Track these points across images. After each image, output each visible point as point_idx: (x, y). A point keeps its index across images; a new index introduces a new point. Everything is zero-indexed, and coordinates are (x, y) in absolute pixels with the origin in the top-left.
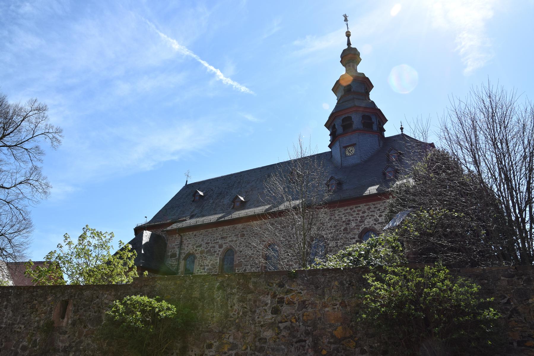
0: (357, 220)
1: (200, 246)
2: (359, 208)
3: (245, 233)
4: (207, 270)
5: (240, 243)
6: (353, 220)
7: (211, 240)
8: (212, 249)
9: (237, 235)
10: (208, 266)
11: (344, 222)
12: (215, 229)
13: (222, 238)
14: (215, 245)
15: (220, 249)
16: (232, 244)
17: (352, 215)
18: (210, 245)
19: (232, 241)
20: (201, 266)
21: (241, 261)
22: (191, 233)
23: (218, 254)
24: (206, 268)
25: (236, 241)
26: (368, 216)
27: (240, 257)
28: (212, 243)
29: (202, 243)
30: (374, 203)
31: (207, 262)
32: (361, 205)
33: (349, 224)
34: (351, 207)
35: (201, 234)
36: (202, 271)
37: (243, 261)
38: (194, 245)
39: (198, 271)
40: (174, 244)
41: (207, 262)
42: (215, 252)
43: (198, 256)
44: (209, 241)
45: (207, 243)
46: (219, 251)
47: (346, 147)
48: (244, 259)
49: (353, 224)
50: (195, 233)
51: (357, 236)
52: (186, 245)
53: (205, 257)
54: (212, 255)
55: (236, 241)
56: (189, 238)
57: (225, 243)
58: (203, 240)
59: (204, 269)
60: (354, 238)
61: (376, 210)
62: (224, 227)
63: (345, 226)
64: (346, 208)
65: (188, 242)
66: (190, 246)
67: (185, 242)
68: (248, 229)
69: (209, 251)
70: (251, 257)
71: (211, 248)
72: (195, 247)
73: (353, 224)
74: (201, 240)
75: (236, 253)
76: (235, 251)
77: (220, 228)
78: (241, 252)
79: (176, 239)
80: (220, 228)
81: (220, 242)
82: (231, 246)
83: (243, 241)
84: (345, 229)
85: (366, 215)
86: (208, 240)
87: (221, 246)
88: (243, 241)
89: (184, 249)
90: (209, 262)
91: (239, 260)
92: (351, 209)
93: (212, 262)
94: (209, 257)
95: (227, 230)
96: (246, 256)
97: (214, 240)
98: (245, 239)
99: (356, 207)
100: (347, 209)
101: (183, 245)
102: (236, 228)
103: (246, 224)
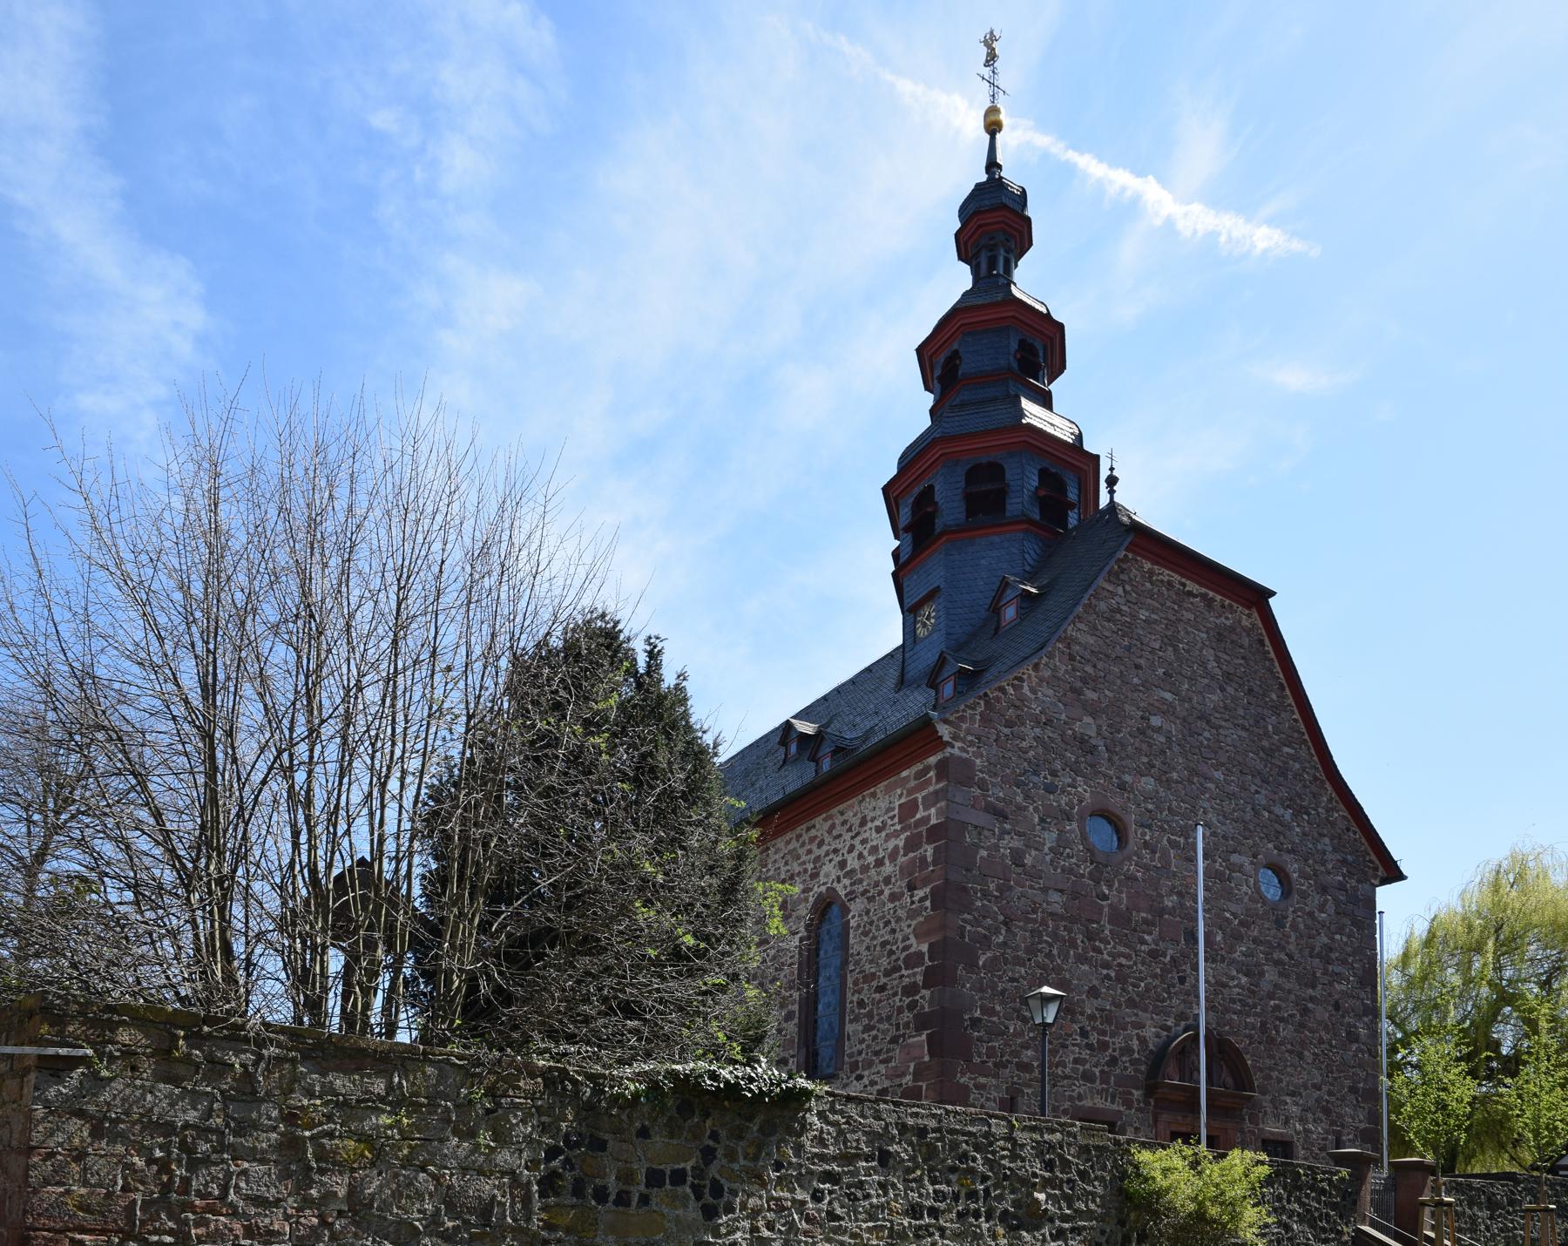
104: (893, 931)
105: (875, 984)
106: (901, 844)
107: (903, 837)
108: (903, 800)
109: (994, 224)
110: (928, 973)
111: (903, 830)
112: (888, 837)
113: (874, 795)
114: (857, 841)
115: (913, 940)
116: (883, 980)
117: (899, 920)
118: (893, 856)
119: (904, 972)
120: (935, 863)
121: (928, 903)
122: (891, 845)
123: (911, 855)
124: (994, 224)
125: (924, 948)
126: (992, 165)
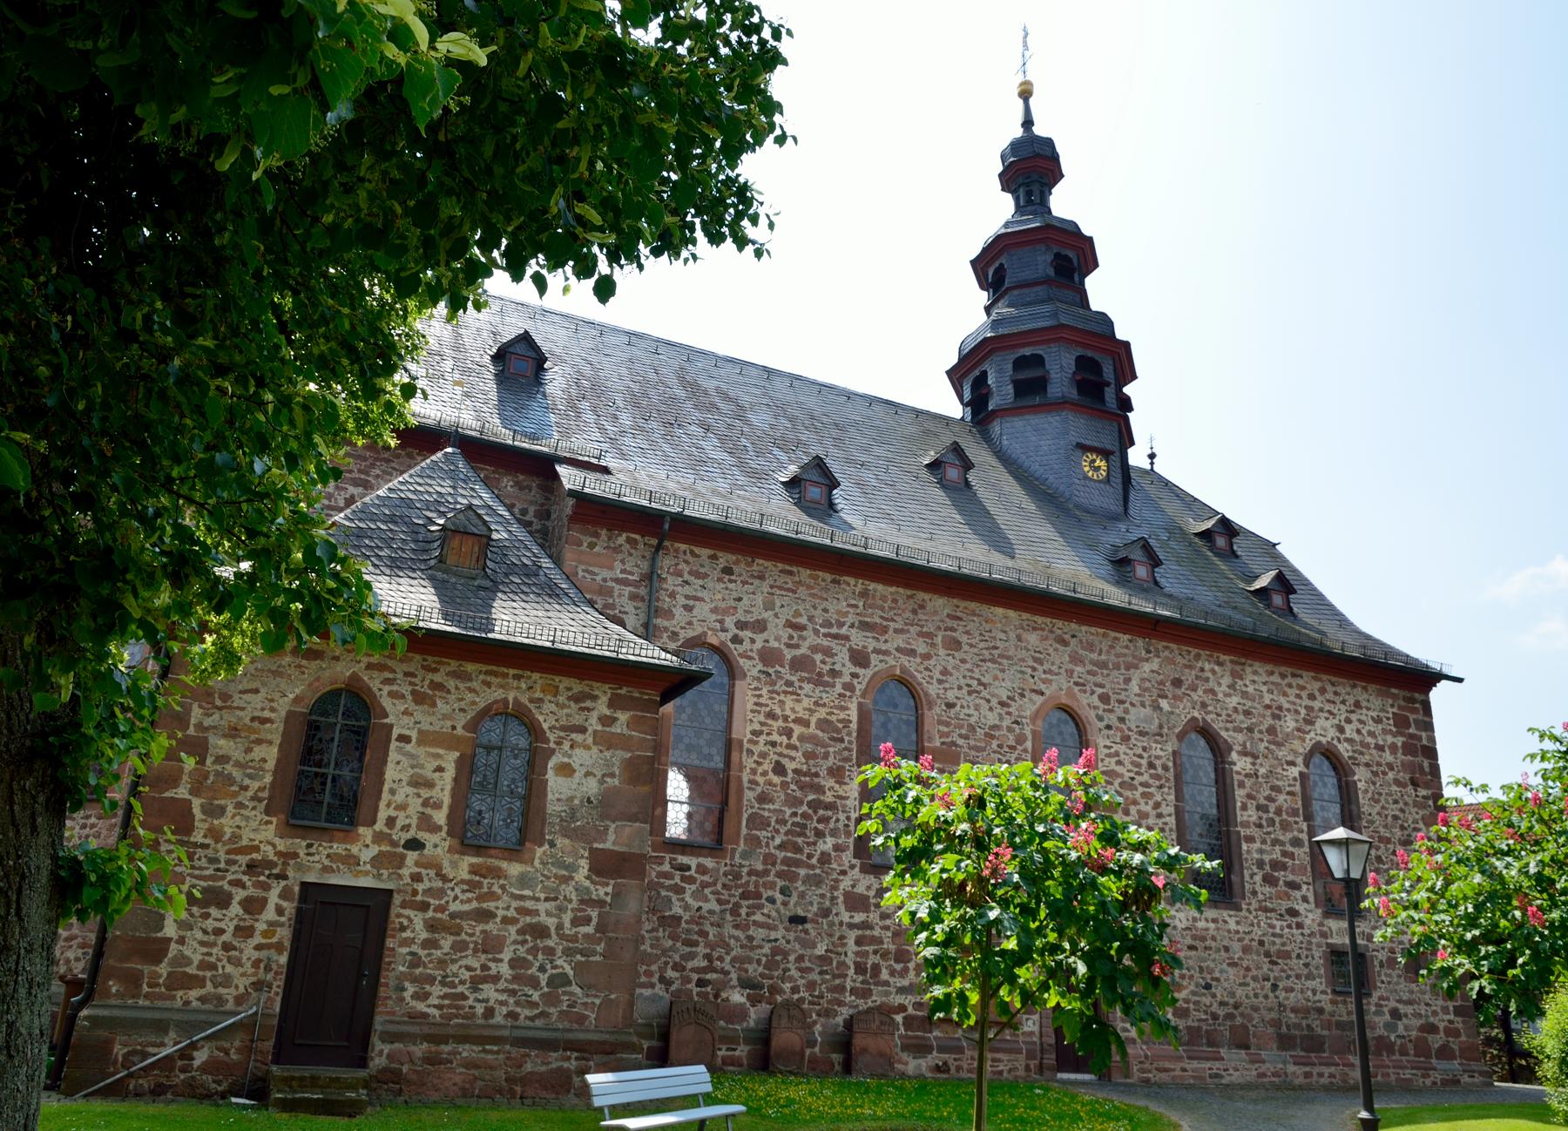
0: (1297, 712)
1: (760, 626)
2: (1301, 682)
3: (964, 639)
4: (801, 738)
5: (945, 672)
6: (1288, 710)
7: (811, 619)
8: (818, 657)
9: (930, 635)
10: (806, 724)
11: (1268, 707)
12: (829, 577)
13: (865, 626)
14: (833, 644)
15: (861, 671)
16: (912, 664)
17: (1285, 694)
18: (811, 639)
19: (912, 653)
20: (771, 715)
21: (954, 744)
22: (705, 552)
23: (849, 687)
24: (798, 730)
25: (927, 657)
26: (1321, 710)
27: (947, 724)
28: (816, 632)
29: (768, 615)
30: (1334, 679)
31: (798, 708)
32: (1305, 673)
33: (1278, 717)
34: (1283, 669)
35: (762, 578)
36: (775, 737)
37: (960, 742)
38: (726, 612)
39: (755, 733)
40: (606, 574)
41: (798, 708)
42: (834, 673)
43: (752, 667)
44: (803, 620)
45: (790, 625)
46: (855, 675)
47: (1085, 448)
48: (966, 737)
49: (1289, 723)
50: (725, 559)
51: (1300, 760)
52: (681, 600)
53: (789, 684)
54: (818, 681)
55: (927, 657)
56: (698, 575)
57: (877, 651)
58: (769, 606)
59: (788, 733)
60: (1293, 764)
61: (1338, 699)
62: (872, 586)
63: (1269, 721)
64: (1269, 667)
65: (687, 590)
66: (702, 610)
67: (671, 583)
68: (971, 626)
69: (798, 664)
70: (993, 737)
71: (815, 649)
72: (730, 622)
73: (1289, 723)
74: (759, 600)
75: (931, 705)
76: (926, 694)
77: (852, 581)
78: (950, 706)
79: (617, 550)
80: (854, 584)
81: (858, 639)
82: (903, 669)
83: (956, 668)
84: (1271, 730)
85: (1316, 704)
86: (797, 614)
87: (860, 658)
88: (956, 668)
89: (669, 614)
90: (812, 711)
91: (942, 735)
92: (1283, 676)
93: (822, 713)
94: (808, 687)
95: (884, 598)
96: (972, 728)
97: (830, 625)
98: (963, 661)
99: (1294, 675)
100: (1272, 673)
101: (663, 595)
102: (922, 607)
103: (963, 604)
109: (1031, 167)
113: (1365, 688)
114: (1354, 717)
117: (1406, 804)
124: (1031, 167)
126: (1028, 123)
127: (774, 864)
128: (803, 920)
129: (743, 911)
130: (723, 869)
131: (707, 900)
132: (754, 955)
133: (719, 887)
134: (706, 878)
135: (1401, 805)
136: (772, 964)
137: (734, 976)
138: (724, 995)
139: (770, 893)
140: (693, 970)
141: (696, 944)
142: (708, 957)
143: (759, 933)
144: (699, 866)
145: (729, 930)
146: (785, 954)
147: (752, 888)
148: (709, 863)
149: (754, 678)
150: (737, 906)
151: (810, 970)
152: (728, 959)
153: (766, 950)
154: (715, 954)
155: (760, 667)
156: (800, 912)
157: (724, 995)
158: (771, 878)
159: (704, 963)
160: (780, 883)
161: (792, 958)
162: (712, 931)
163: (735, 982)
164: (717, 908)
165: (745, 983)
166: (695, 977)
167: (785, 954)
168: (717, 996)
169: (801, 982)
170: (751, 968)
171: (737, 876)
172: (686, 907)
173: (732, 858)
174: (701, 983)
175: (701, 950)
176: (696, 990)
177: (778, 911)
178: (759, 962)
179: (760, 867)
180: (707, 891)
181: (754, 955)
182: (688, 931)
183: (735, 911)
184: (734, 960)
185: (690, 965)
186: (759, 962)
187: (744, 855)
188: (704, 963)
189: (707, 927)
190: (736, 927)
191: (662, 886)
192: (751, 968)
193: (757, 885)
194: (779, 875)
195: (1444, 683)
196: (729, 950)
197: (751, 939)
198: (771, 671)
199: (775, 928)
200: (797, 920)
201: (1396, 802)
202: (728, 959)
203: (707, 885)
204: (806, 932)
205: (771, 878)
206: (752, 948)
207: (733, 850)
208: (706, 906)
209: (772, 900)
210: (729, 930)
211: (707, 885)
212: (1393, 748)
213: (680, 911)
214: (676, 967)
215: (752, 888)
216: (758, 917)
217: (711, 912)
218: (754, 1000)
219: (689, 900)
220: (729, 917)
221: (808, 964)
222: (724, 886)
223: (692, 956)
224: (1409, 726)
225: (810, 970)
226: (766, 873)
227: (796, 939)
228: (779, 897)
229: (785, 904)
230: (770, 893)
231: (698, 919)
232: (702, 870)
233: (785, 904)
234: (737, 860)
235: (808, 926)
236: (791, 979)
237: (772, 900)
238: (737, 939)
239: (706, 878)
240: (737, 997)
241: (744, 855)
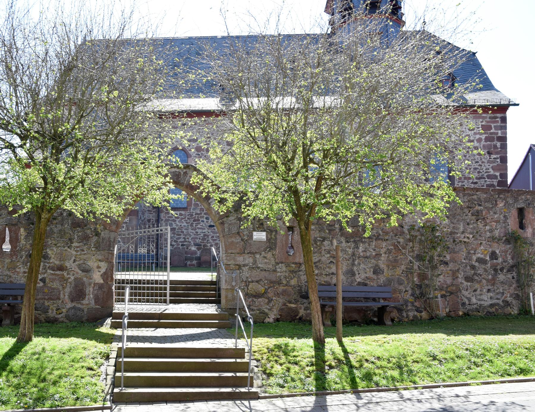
104: (481, 165)
105: (471, 181)
106: (483, 138)
107: (485, 136)
108: (483, 124)
110: (499, 182)
111: (485, 133)
112: (475, 134)
115: (491, 170)
116: (475, 181)
117: (483, 162)
118: (479, 140)
119: (486, 179)
120: (501, 148)
121: (499, 160)
122: (478, 136)
123: (488, 143)
125: (498, 174)
127: (203, 211)
128: (213, 226)
129: (194, 225)
130: (187, 214)
131: (183, 223)
132: (198, 237)
133: (186, 219)
134: (182, 217)
135: (480, 163)
136: (204, 239)
137: (192, 243)
138: (189, 248)
139: (202, 219)
140: (180, 242)
141: (181, 235)
142: (184, 238)
143: (200, 231)
144: (180, 214)
145: (190, 230)
146: (208, 236)
147: (196, 218)
148: (183, 212)
149: (194, 157)
150: (192, 223)
151: (215, 240)
152: (190, 238)
153: (202, 235)
154: (186, 237)
155: (196, 153)
156: (212, 224)
157: (189, 248)
158: (203, 215)
159: (183, 240)
160: (205, 216)
161: (210, 237)
162: (185, 231)
163: (193, 244)
164: (186, 225)
165: (196, 245)
166: (181, 244)
167: (208, 236)
168: (187, 248)
169: (213, 243)
170: (197, 240)
171: (192, 215)
172: (177, 225)
173: (190, 210)
174: (182, 245)
175: (182, 236)
176: (181, 247)
177: (205, 224)
178: (200, 239)
179: (199, 212)
180: (183, 220)
181: (198, 237)
182: (178, 232)
183: (192, 225)
184: (192, 239)
185: (179, 241)
186: (200, 239)
187: (194, 209)
188: (183, 240)
189: (184, 230)
190: (192, 229)
191: (169, 220)
192: (197, 240)
193: (198, 217)
194: (205, 214)
195: (510, 107)
196: (190, 236)
197: (197, 232)
198: (200, 153)
199: (204, 229)
200: (211, 226)
201: (477, 162)
202: (190, 238)
203: (183, 219)
204: (214, 229)
205: (203, 215)
206: (198, 235)
207: (190, 208)
208: (183, 225)
209: (203, 221)
210: (190, 230)
211: (183, 219)
212: (479, 140)
213: (175, 227)
214: (175, 241)
215: (196, 218)
216: (199, 226)
217: (184, 226)
218: (198, 249)
219: (178, 223)
220: (190, 227)
221: (215, 238)
222: (188, 218)
223: (180, 238)
224: (491, 129)
225: (215, 240)
226: (201, 213)
227: (211, 232)
228: (205, 220)
229: (207, 222)
230: (202, 219)
231: (181, 228)
232: (181, 215)
233: (207, 222)
234: (192, 211)
235: (215, 228)
236: (210, 242)
237: (203, 221)
238: (193, 233)
239: (182, 217)
240: (193, 248)
241: (194, 209)
